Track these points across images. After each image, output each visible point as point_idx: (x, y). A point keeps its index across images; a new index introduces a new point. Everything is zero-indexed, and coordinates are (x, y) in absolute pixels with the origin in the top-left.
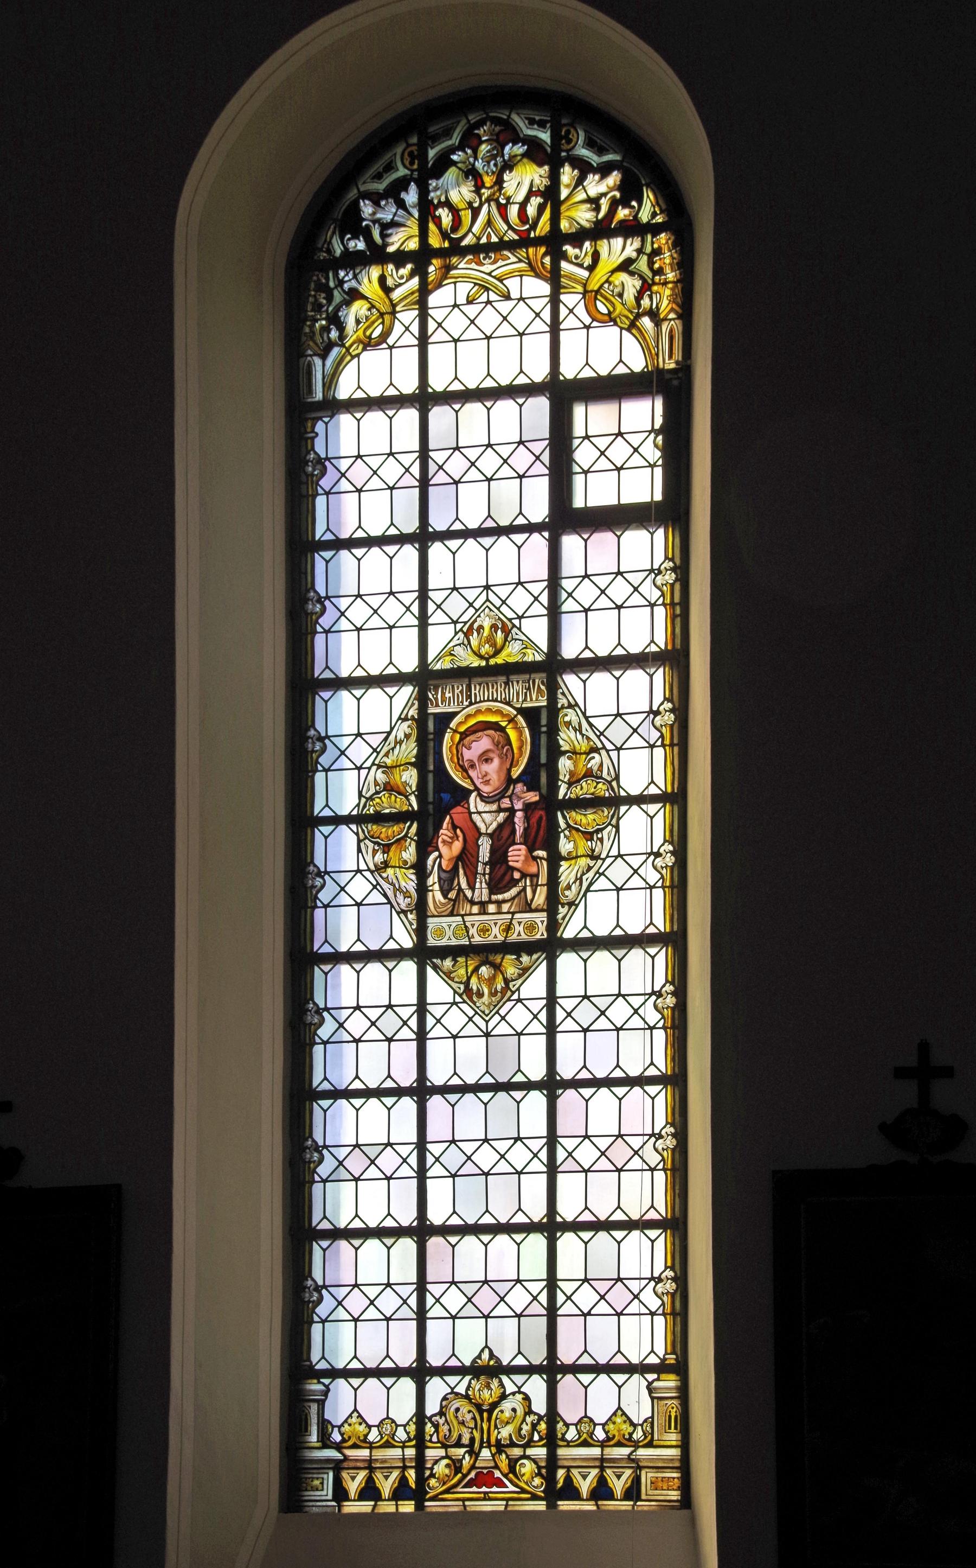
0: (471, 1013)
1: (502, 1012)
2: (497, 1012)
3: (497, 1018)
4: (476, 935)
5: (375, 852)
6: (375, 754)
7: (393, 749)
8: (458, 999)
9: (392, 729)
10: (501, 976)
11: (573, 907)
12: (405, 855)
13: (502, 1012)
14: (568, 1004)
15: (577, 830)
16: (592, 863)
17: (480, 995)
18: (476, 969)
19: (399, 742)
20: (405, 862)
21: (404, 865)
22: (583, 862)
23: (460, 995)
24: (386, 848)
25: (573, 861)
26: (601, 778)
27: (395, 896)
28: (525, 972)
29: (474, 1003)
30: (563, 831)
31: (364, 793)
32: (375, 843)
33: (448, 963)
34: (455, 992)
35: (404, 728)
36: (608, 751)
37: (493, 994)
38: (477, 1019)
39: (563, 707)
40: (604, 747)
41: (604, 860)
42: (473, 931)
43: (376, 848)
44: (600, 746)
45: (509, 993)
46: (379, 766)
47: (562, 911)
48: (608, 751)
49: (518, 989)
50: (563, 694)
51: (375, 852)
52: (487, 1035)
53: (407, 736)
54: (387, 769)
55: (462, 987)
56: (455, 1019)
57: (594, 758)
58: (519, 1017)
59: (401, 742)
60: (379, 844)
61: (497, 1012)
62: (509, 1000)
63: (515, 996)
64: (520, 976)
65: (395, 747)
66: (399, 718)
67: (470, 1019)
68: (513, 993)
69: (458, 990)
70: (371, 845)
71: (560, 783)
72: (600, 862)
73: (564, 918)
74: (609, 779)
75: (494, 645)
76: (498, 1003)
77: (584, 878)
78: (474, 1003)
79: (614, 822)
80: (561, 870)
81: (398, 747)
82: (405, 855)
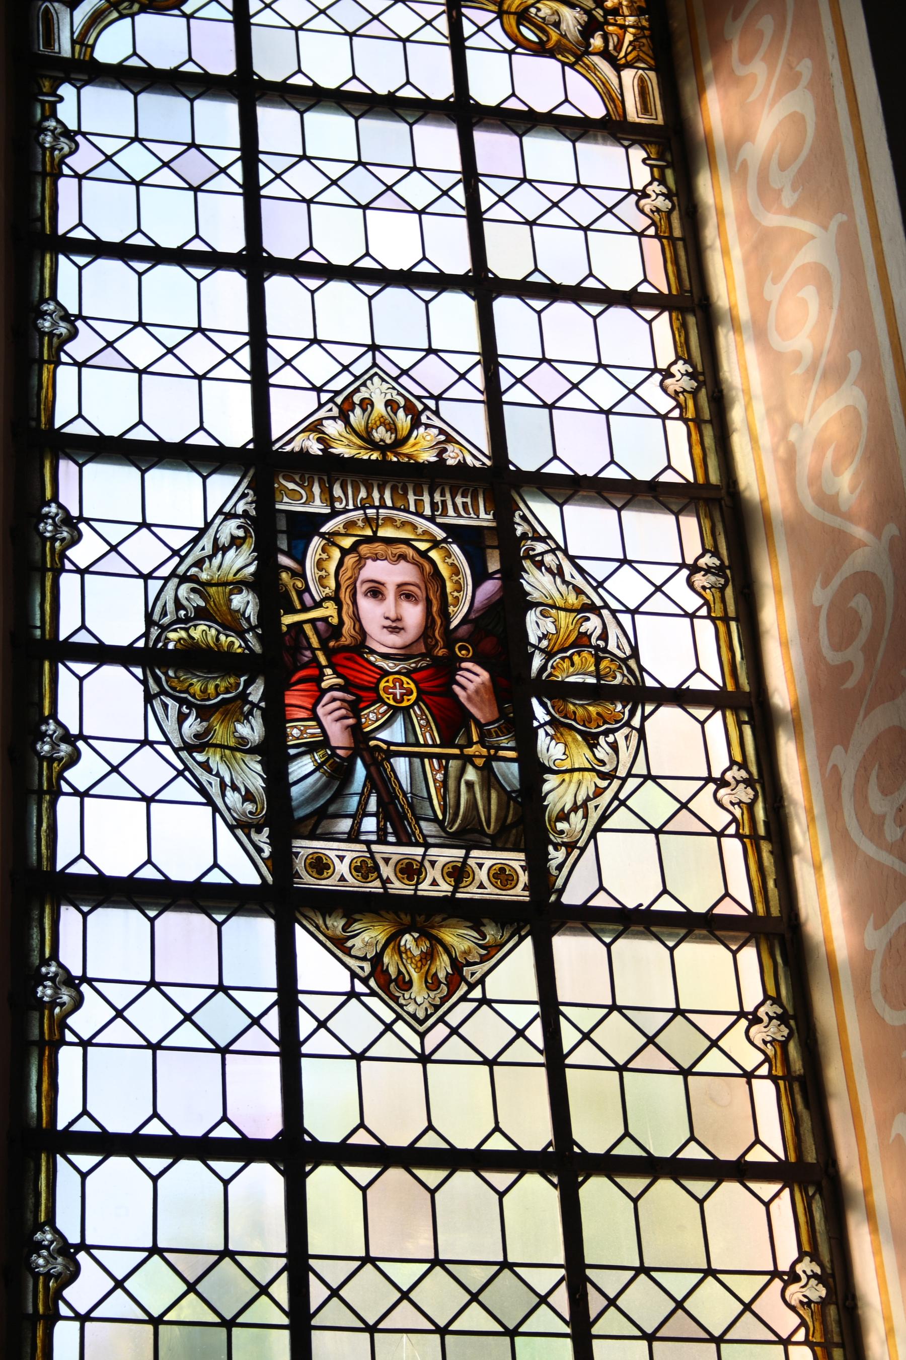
0: (389, 1016)
1: (454, 1018)
4: (393, 878)
5: (182, 718)
6: (176, 560)
7: (210, 558)
8: (360, 987)
9: (208, 525)
10: (445, 958)
11: (576, 852)
12: (243, 730)
13: (454, 1018)
14: (586, 1018)
15: (571, 728)
16: (603, 784)
17: (408, 985)
18: (393, 939)
19: (218, 548)
20: (243, 740)
21: (242, 746)
22: (590, 781)
23: (365, 981)
24: (204, 713)
25: (567, 776)
26: (605, 650)
27: (223, 795)
28: (491, 952)
29: (396, 999)
30: (541, 726)
31: (156, 617)
32: (181, 701)
33: (337, 924)
34: (354, 975)
35: (231, 528)
36: (613, 612)
37: (432, 983)
38: (400, 1027)
39: (524, 536)
40: (606, 606)
41: (624, 780)
42: (387, 871)
43: (185, 710)
44: (599, 603)
45: (464, 988)
46: (184, 579)
47: (557, 856)
48: (613, 612)
49: (482, 981)
50: (524, 518)
51: (182, 718)
53: (235, 542)
54: (201, 587)
55: (367, 967)
57: (588, 619)
58: (487, 1031)
59: (225, 550)
60: (190, 706)
61: (441, 1020)
62: (464, 998)
63: (477, 993)
64: (483, 959)
65: (214, 554)
66: (220, 512)
67: (388, 1027)
68: (472, 987)
69: (358, 971)
70: (173, 705)
71: (530, 650)
72: (616, 783)
73: (560, 867)
74: (622, 655)
75: (392, 428)
76: (444, 1000)
77: (591, 805)
78: (396, 999)
79: (636, 722)
80: (546, 787)
81: (220, 555)
82: (243, 730)
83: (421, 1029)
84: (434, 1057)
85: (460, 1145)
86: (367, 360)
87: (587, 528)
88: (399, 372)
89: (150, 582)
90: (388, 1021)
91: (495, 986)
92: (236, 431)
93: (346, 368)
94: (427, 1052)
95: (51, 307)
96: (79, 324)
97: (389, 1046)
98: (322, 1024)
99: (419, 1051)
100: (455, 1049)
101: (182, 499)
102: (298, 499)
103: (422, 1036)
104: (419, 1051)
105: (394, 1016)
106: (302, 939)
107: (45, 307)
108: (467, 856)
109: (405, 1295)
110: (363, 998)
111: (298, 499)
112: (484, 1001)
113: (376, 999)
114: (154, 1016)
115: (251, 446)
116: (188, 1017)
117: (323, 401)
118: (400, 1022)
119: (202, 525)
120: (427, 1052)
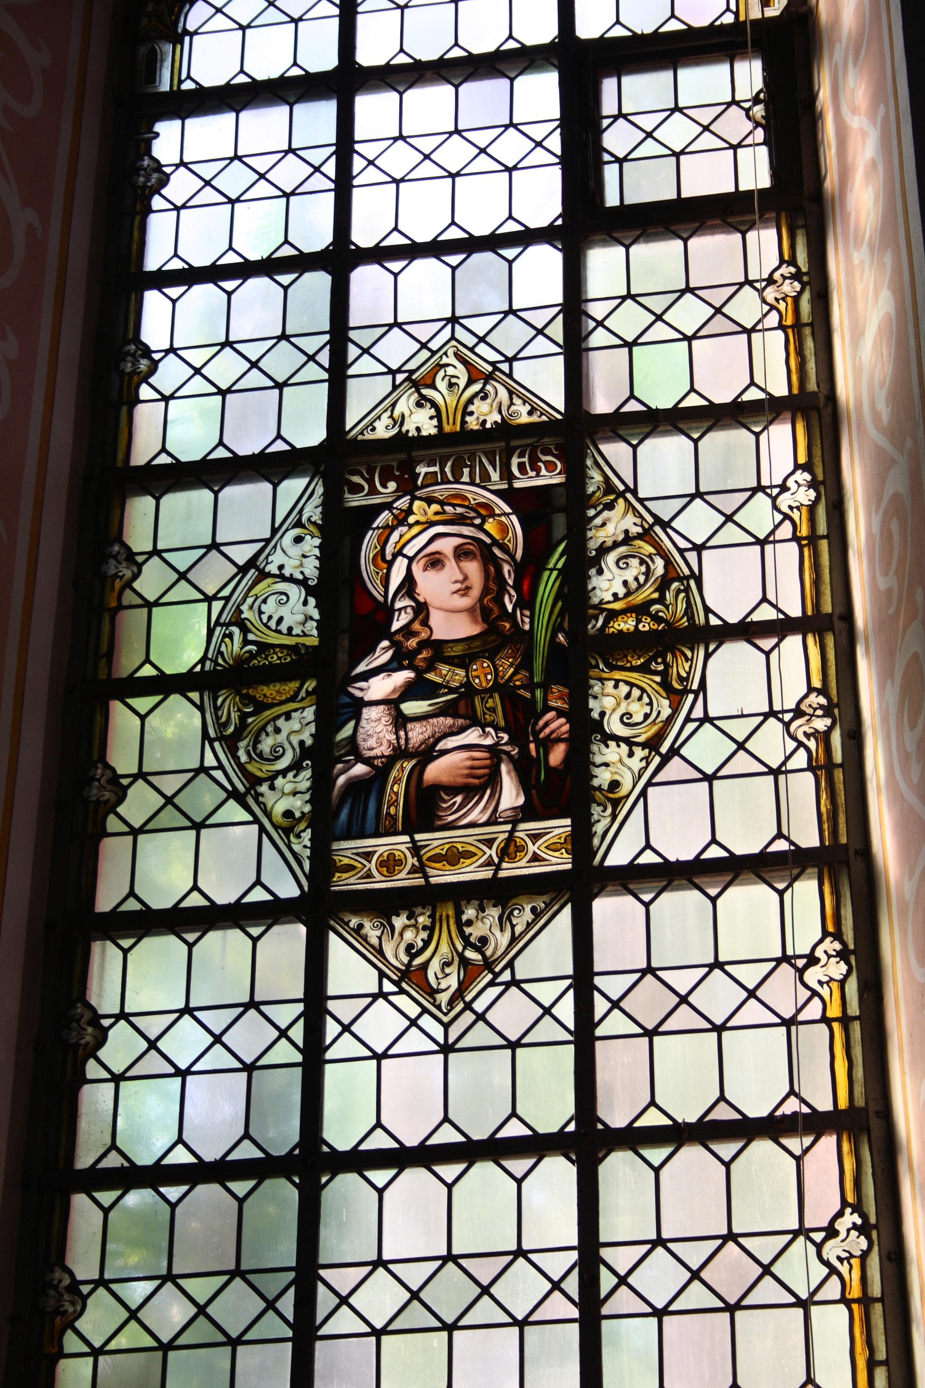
1: (479, 1006)
38: (426, 1022)
52: (446, 1049)
56: (381, 1024)
58: (512, 1013)
85: (752, 1114)
86: (446, 333)
87: (662, 465)
88: (476, 340)
90: (413, 1016)
97: (414, 1041)
98: (616, 1005)
99: (442, 1042)
100: (481, 1035)
105: (419, 1010)
106: (336, 945)
109: (485, 1290)
110: (391, 998)
112: (515, 983)
113: (404, 997)
114: (717, 998)
116: (684, 1000)
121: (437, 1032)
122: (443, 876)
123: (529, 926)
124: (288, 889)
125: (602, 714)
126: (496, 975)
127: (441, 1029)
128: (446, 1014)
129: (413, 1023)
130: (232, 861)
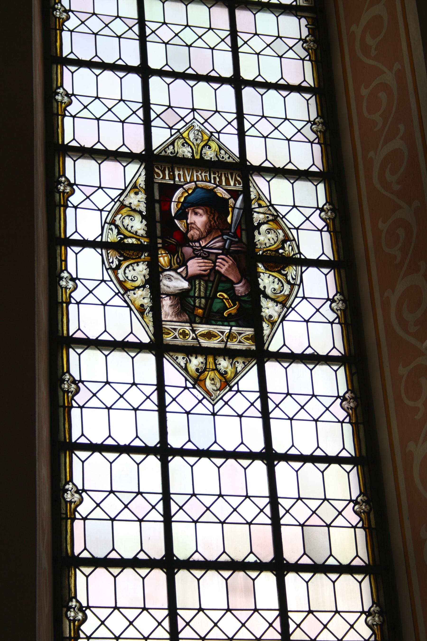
1: (226, 398)
2: (221, 398)
3: (221, 403)
6: (113, 203)
13: (226, 398)
52: (214, 414)
58: (239, 403)
83: (213, 403)
84: (218, 414)
89: (103, 212)
91: (243, 385)
92: (138, 147)
93: (182, 119)
94: (215, 412)
95: (63, 179)
96: (73, 98)
100: (226, 410)
101: (116, 175)
102: (163, 177)
103: (213, 405)
104: (212, 411)
107: (58, 91)
108: (231, 330)
111: (163, 177)
112: (238, 391)
115: (144, 153)
117: (172, 134)
118: (205, 400)
119: (124, 188)
120: (215, 412)
121: (210, 407)
122: (205, 343)
123: (243, 369)
124: (146, 340)
125: (265, 287)
126: (231, 387)
127: (211, 406)
128: (213, 400)
129: (200, 401)
130: (122, 323)
